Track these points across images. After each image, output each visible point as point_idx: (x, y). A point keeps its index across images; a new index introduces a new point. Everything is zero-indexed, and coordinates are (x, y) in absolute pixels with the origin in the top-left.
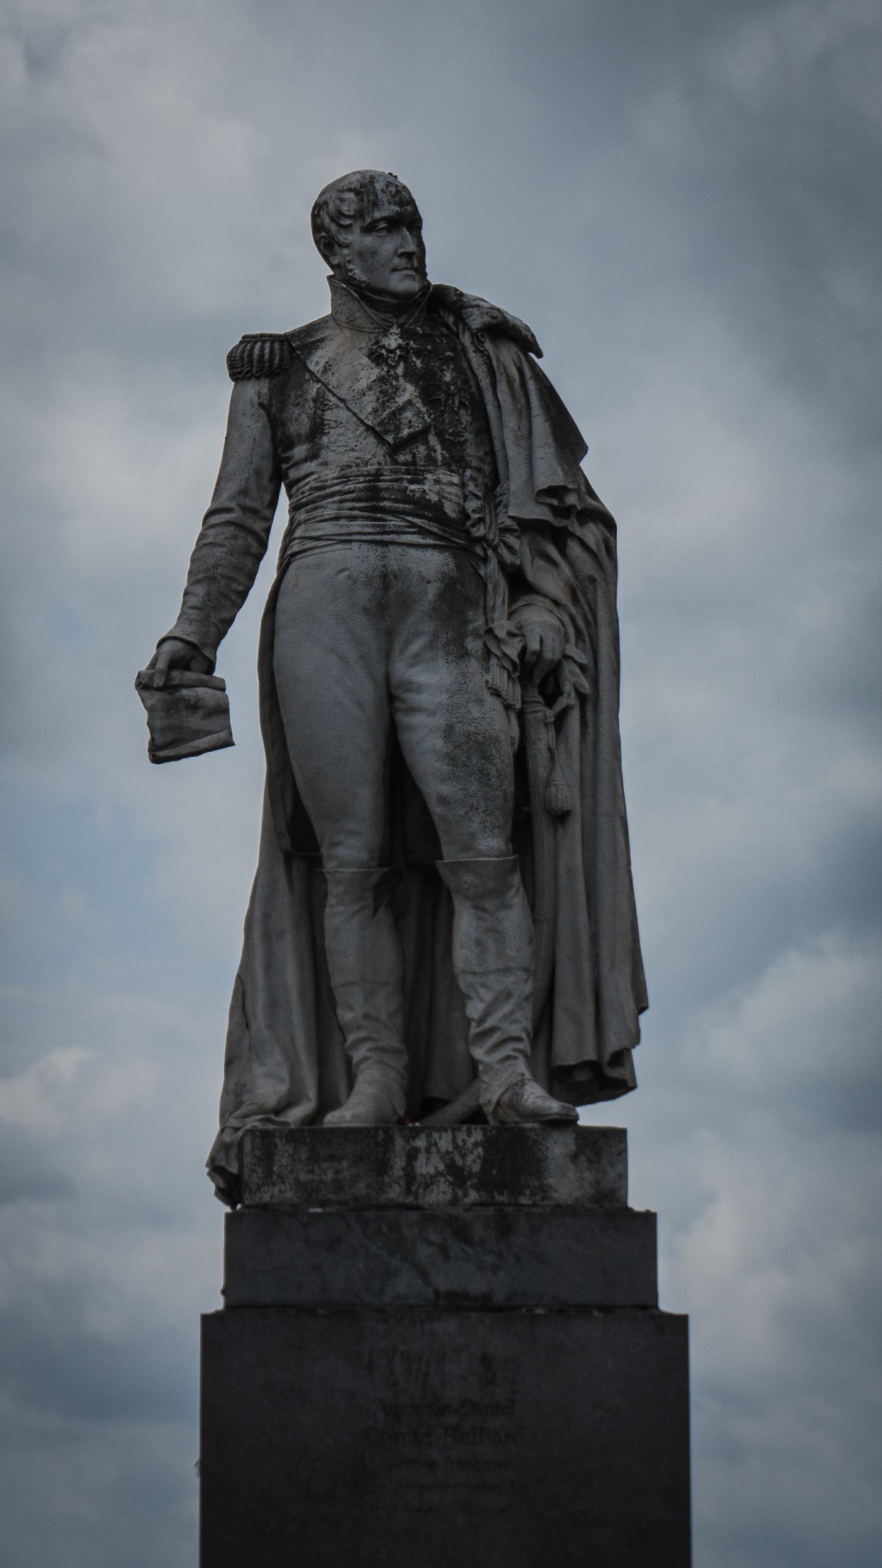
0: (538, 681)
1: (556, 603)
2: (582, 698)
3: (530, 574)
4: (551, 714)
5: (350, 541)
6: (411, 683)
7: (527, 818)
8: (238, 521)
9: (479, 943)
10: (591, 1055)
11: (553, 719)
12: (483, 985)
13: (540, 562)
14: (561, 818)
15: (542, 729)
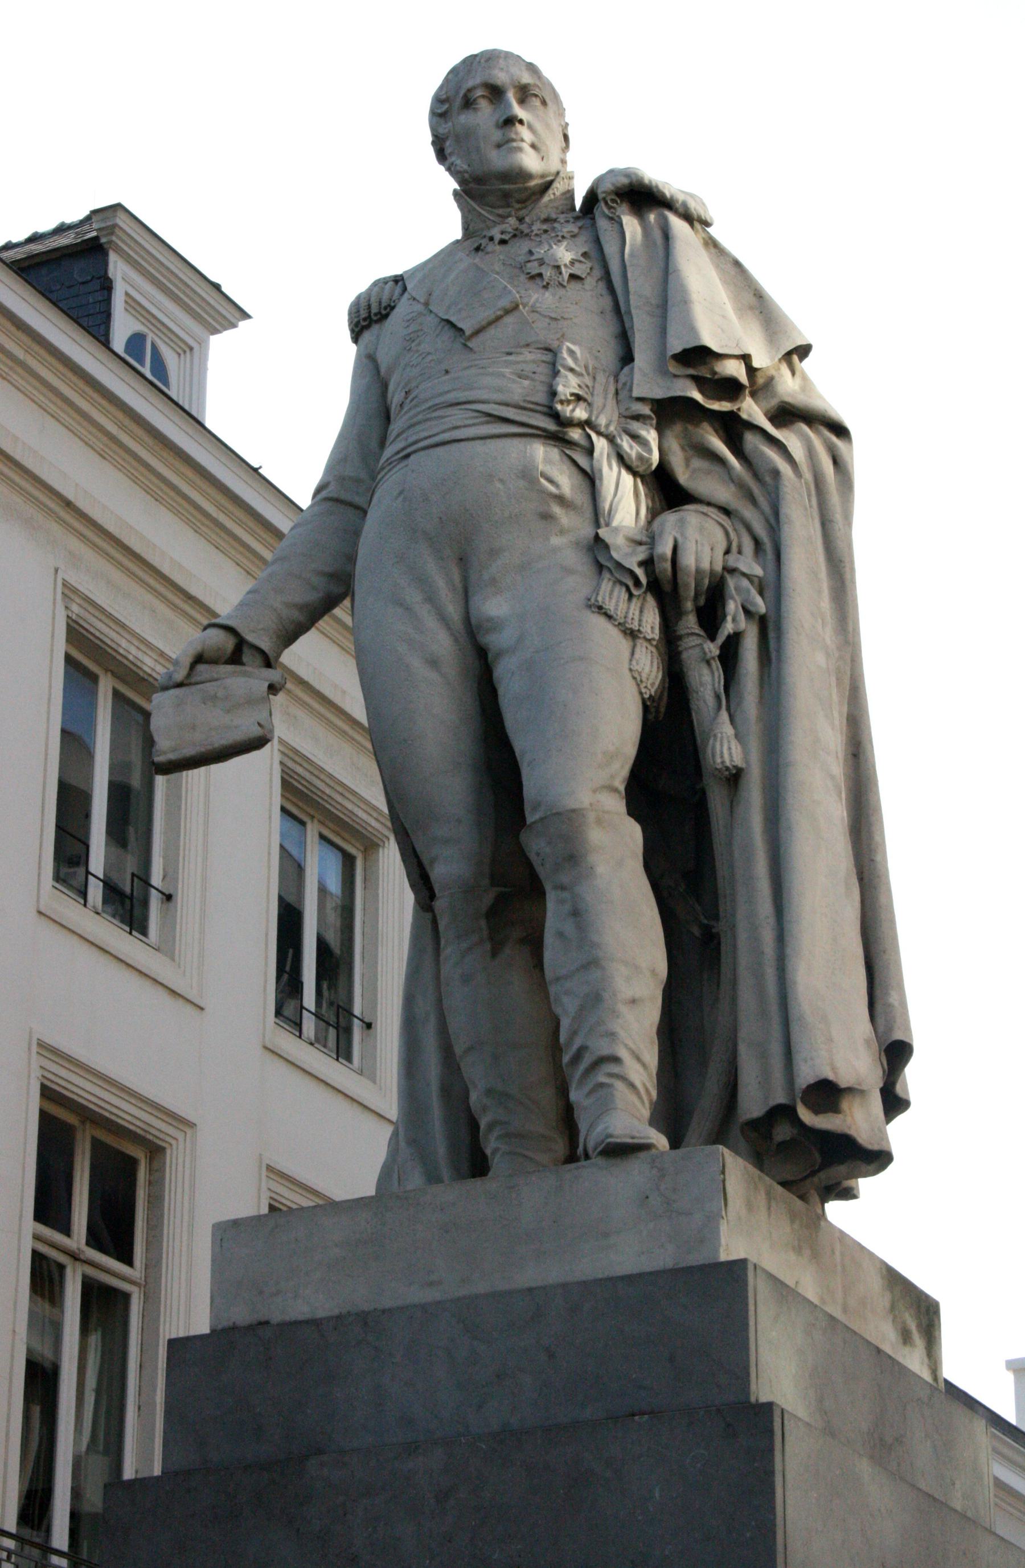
0: (689, 605)
1: (726, 511)
2: (763, 623)
3: (682, 477)
4: (713, 649)
5: (407, 456)
6: (490, 619)
7: (675, 786)
8: (335, 495)
9: (560, 935)
10: (780, 1098)
11: (718, 652)
12: (567, 993)
13: (697, 463)
14: (734, 778)
15: (705, 671)
